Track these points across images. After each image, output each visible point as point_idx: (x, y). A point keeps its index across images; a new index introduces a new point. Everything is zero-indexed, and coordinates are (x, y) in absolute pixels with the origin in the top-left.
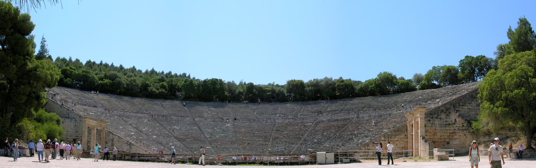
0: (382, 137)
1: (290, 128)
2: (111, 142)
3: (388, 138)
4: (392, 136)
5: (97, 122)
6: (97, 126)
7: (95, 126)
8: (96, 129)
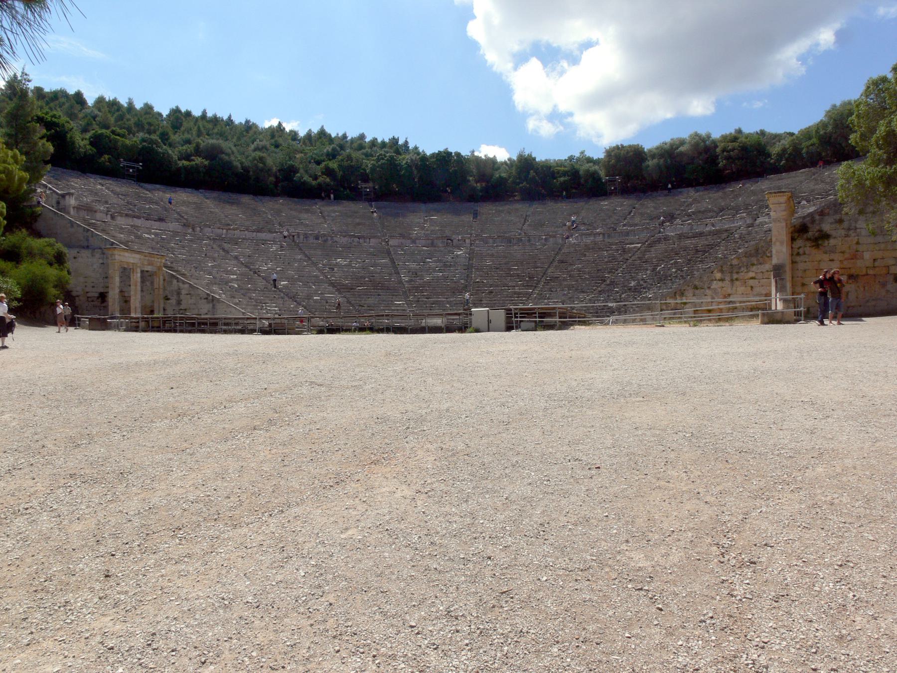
0: (715, 272)
1: (590, 256)
2: (175, 297)
3: (731, 273)
6: (143, 264)
7: (138, 265)
8: (139, 271)
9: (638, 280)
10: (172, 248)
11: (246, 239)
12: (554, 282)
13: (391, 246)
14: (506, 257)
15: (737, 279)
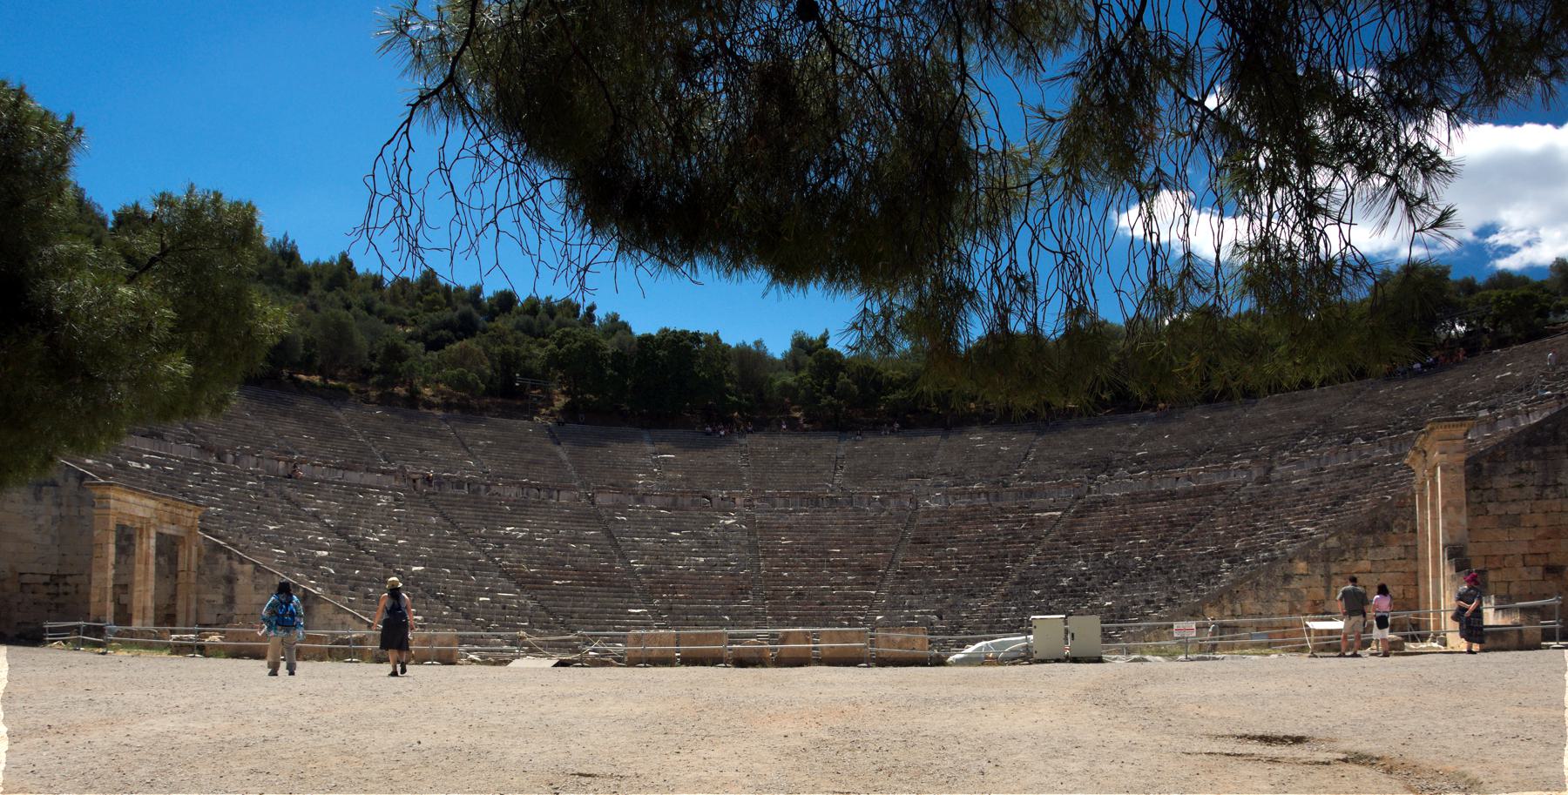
2: (222, 588)
4: (1343, 552)
5: (160, 506)
7: (153, 521)
8: (153, 533)
9: (1074, 575)
10: (193, 492)
11: (328, 482)
12: (913, 578)
13: (602, 507)
14: (816, 532)
15: (1336, 574)
